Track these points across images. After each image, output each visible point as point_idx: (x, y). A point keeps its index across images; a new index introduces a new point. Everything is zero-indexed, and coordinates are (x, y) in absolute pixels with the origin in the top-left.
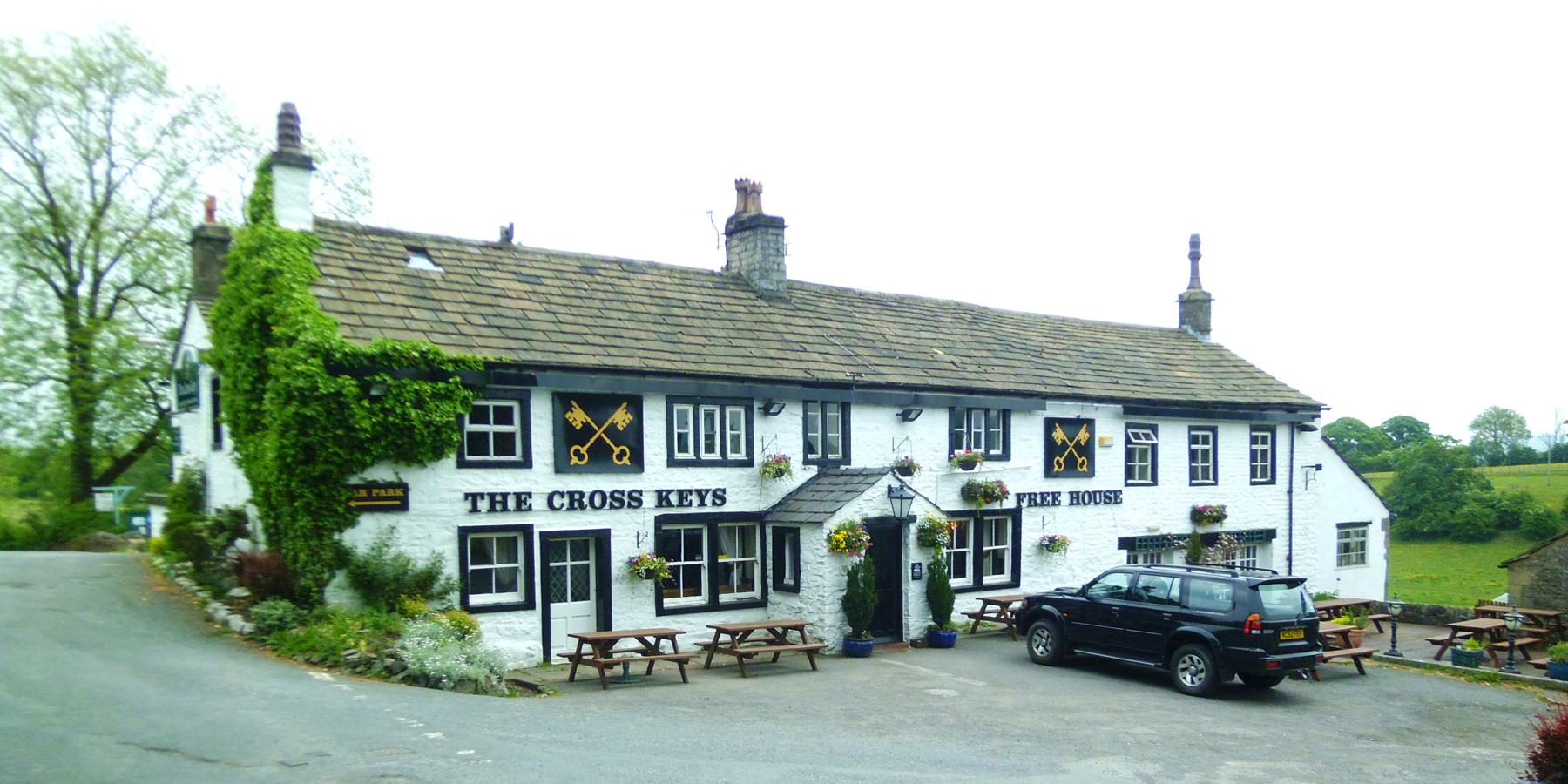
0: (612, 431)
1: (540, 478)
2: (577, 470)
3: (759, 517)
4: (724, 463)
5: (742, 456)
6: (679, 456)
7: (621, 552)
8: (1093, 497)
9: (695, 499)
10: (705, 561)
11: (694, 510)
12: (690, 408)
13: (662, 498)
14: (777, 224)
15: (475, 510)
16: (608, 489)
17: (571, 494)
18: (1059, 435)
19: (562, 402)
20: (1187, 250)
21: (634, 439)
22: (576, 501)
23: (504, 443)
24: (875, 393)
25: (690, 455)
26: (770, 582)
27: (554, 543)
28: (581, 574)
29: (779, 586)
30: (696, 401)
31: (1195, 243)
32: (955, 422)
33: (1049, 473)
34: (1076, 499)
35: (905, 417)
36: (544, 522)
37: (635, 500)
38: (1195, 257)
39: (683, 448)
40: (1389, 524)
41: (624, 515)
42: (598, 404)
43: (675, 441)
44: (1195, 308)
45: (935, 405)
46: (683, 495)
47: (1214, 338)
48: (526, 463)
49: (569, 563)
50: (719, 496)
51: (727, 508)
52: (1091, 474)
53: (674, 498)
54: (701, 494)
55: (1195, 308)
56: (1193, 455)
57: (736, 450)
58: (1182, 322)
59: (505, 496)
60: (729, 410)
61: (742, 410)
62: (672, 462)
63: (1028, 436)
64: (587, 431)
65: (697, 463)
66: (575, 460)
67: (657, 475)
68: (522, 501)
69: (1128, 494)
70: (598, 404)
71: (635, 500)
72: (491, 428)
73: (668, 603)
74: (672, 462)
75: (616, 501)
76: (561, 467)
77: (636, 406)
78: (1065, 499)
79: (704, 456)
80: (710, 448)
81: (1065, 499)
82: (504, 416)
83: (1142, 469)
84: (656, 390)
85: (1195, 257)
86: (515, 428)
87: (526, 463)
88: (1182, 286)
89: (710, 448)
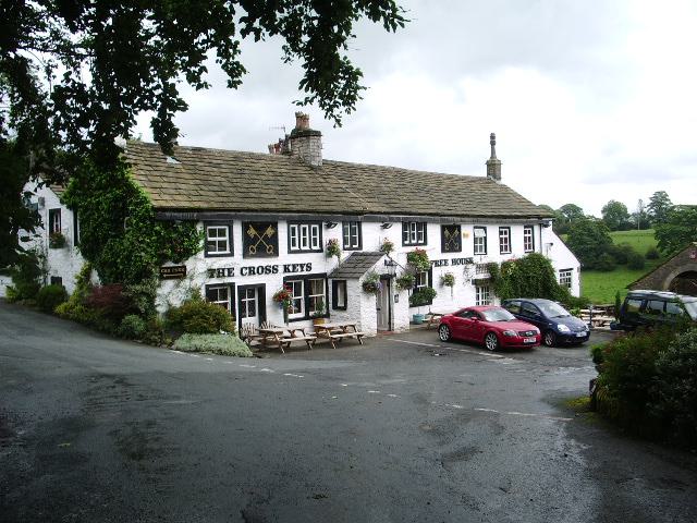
0: (266, 238)
2: (253, 256)
3: (324, 275)
4: (311, 251)
5: (317, 248)
6: (292, 248)
7: (270, 293)
8: (461, 261)
9: (299, 268)
10: (303, 296)
12: (296, 226)
13: (286, 269)
14: (318, 134)
15: (212, 276)
16: (264, 266)
17: (250, 268)
18: (447, 232)
19: (245, 228)
20: (489, 140)
21: (274, 240)
22: (252, 271)
23: (222, 245)
24: (372, 217)
25: (297, 248)
26: (331, 305)
27: (245, 290)
28: (252, 304)
29: (335, 307)
30: (299, 222)
31: (493, 137)
32: (404, 228)
33: (443, 251)
34: (455, 262)
35: (385, 227)
37: (275, 269)
38: (493, 143)
39: (294, 245)
40: (583, 270)
41: (271, 275)
42: (261, 227)
43: (291, 242)
44: (493, 166)
45: (398, 220)
47: (503, 182)
48: (232, 254)
49: (247, 300)
50: (309, 267)
51: (313, 272)
52: (460, 250)
53: (291, 268)
54: (302, 266)
55: (493, 166)
56: (501, 239)
57: (315, 245)
58: (488, 174)
59: (223, 270)
60: (302, 226)
61: (317, 226)
62: (290, 252)
63: (434, 233)
64: (256, 238)
66: (251, 252)
67: (284, 258)
68: (230, 271)
70: (261, 227)
71: (275, 269)
72: (217, 239)
73: (291, 316)
74: (290, 252)
76: (246, 255)
77: (275, 226)
78: (450, 262)
79: (303, 248)
81: (450, 262)
82: (222, 233)
84: (284, 219)
85: (493, 143)
86: (227, 238)
87: (232, 254)
88: (488, 158)
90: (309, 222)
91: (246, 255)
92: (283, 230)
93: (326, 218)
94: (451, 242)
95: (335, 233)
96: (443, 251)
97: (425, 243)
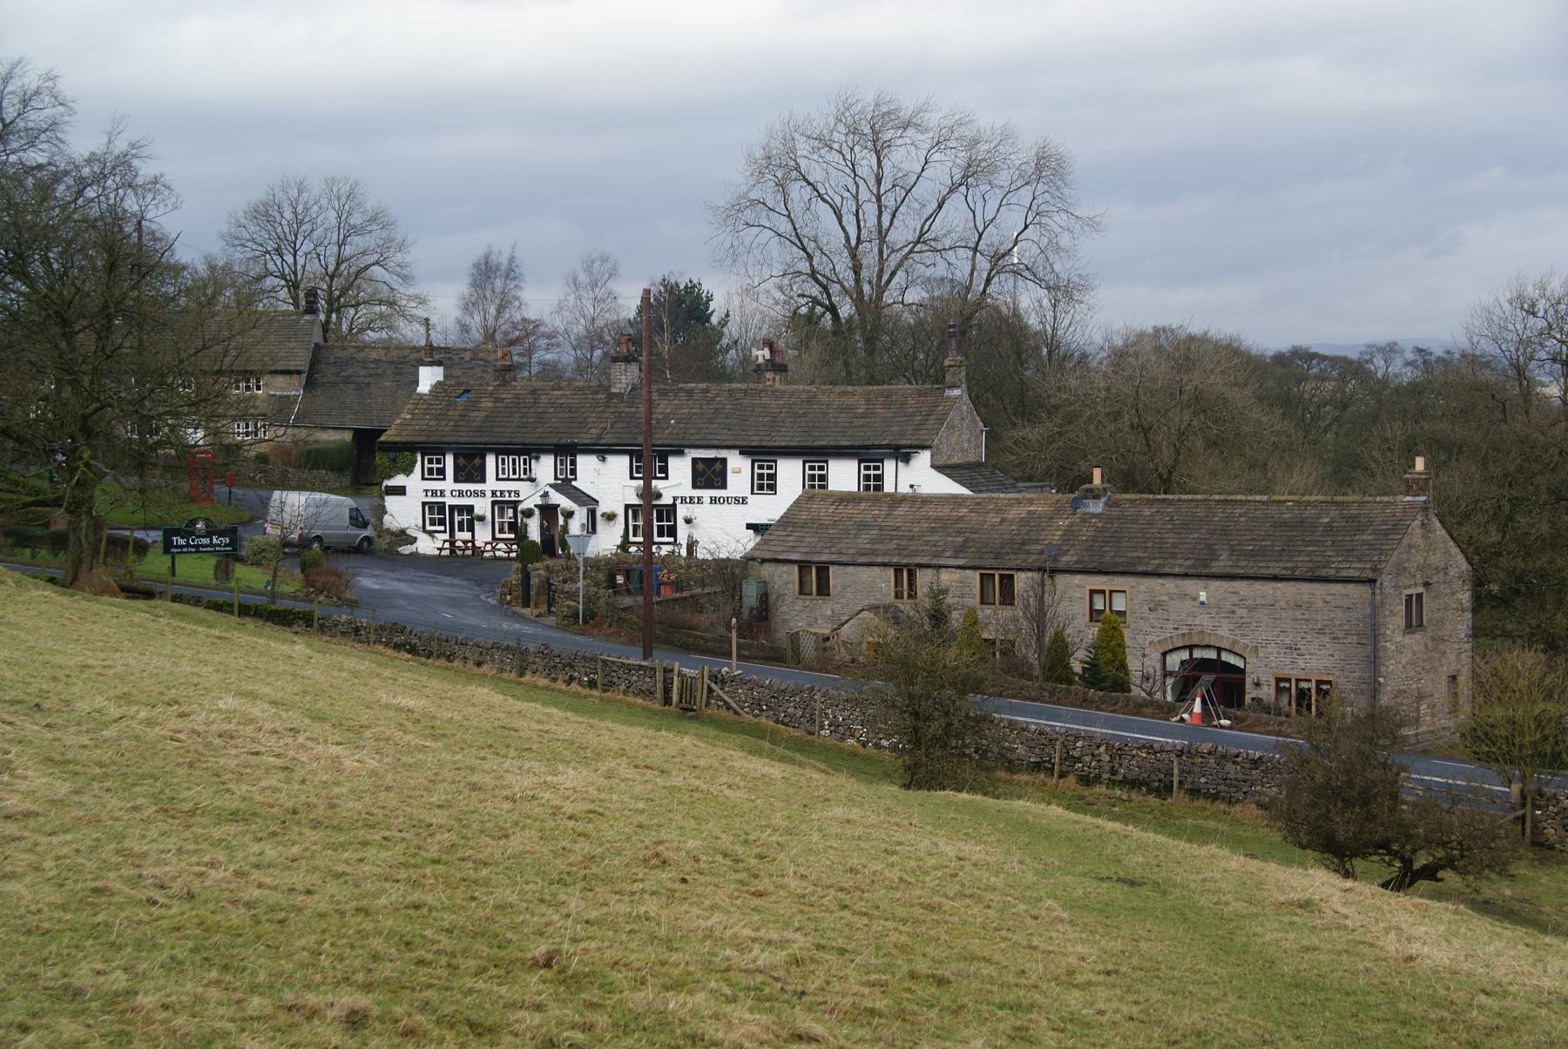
1: (449, 484)
4: (519, 479)
6: (501, 476)
8: (727, 500)
11: (507, 498)
13: (494, 493)
18: (700, 466)
22: (461, 494)
27: (452, 508)
33: (695, 486)
34: (714, 500)
36: (450, 501)
37: (483, 494)
46: (502, 492)
48: (444, 479)
50: (517, 493)
52: (724, 486)
54: (510, 492)
65: (508, 479)
67: (491, 484)
69: (752, 499)
71: (483, 494)
75: (476, 494)
76: (456, 480)
79: (511, 476)
80: (514, 473)
83: (765, 484)
89: (514, 473)
90: (519, 453)
91: (456, 480)
92: (490, 461)
93: (532, 451)
94: (710, 476)
95: (545, 468)
96: (695, 486)
97: (666, 478)
